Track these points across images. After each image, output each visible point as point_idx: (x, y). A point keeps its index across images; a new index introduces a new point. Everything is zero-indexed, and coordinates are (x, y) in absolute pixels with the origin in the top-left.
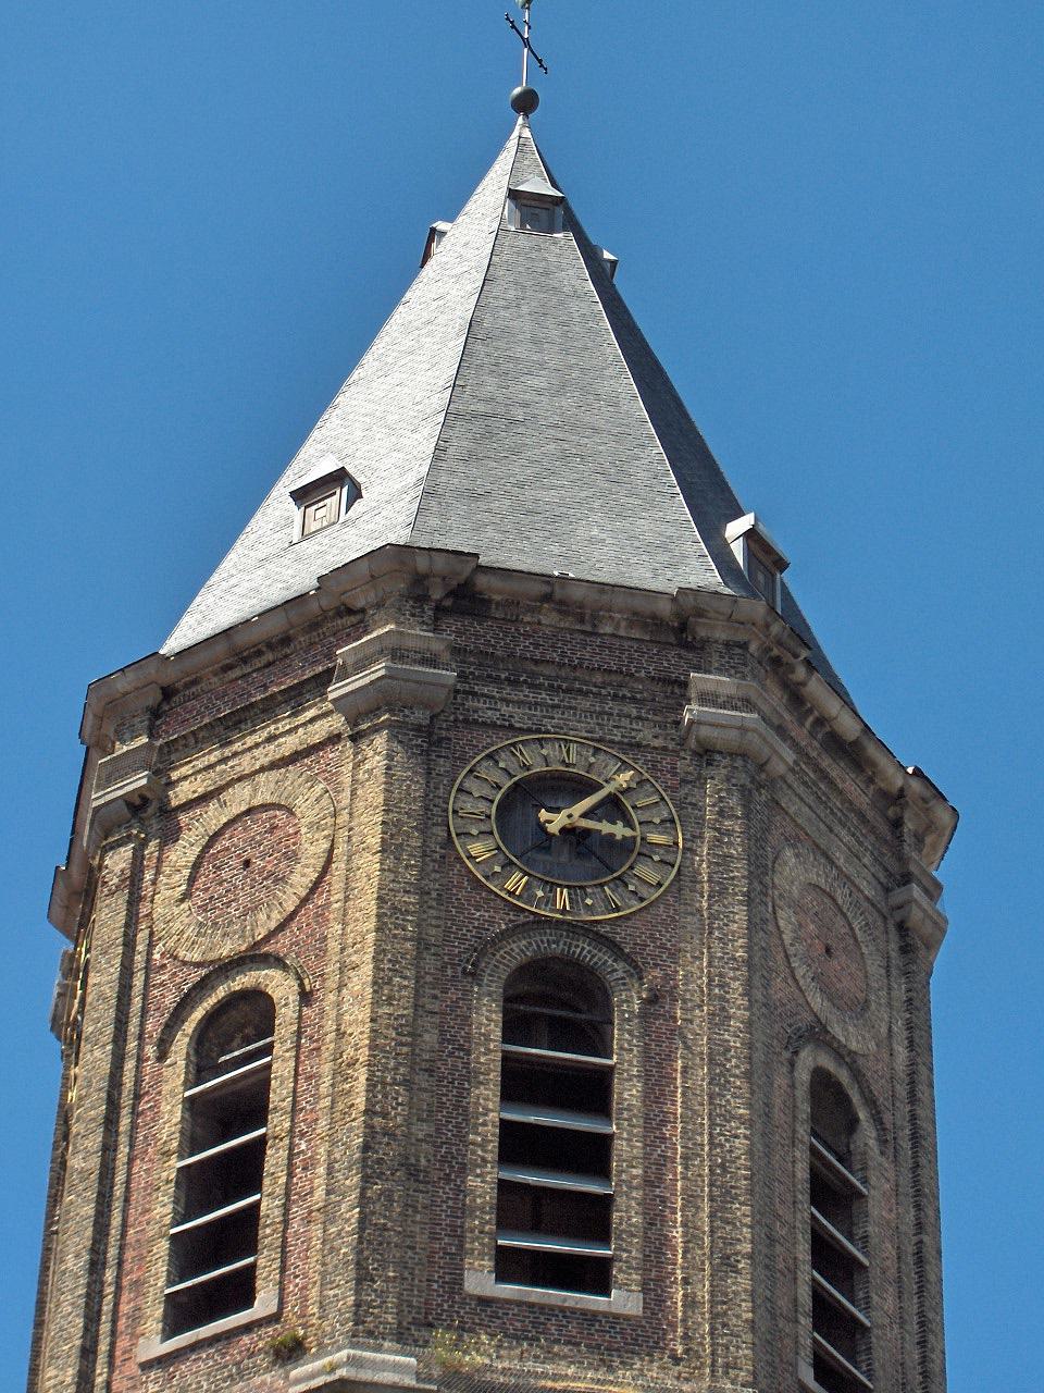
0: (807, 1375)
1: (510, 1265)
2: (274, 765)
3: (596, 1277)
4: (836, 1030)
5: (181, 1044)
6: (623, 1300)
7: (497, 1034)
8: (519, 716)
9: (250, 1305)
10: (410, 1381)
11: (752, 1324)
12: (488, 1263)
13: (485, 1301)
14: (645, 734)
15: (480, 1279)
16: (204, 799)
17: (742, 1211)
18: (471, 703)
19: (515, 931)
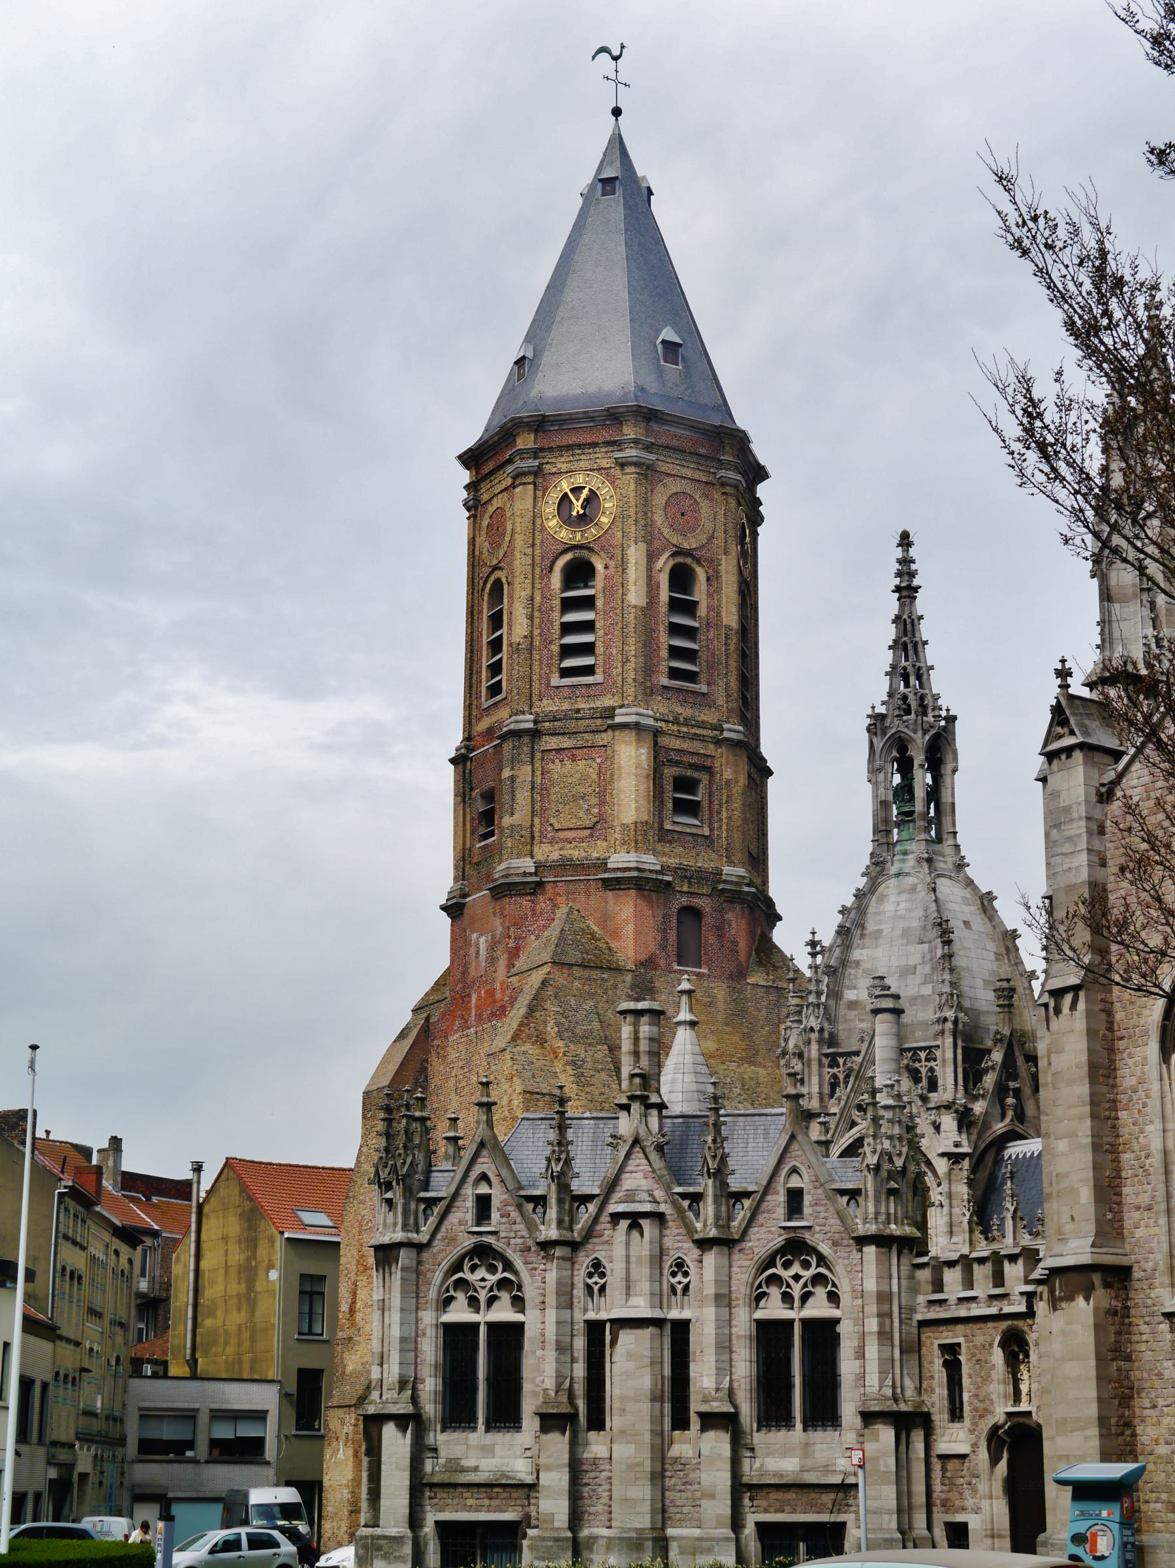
0: (665, 681)
1: (566, 673)
2: (502, 491)
3: (589, 670)
4: (686, 546)
5: (486, 598)
6: (598, 678)
7: (558, 591)
8: (564, 467)
9: (500, 692)
10: (531, 725)
11: (635, 680)
12: (557, 675)
13: (557, 687)
14: (605, 463)
15: (556, 680)
16: (490, 500)
17: (631, 641)
18: (548, 466)
19: (565, 551)
